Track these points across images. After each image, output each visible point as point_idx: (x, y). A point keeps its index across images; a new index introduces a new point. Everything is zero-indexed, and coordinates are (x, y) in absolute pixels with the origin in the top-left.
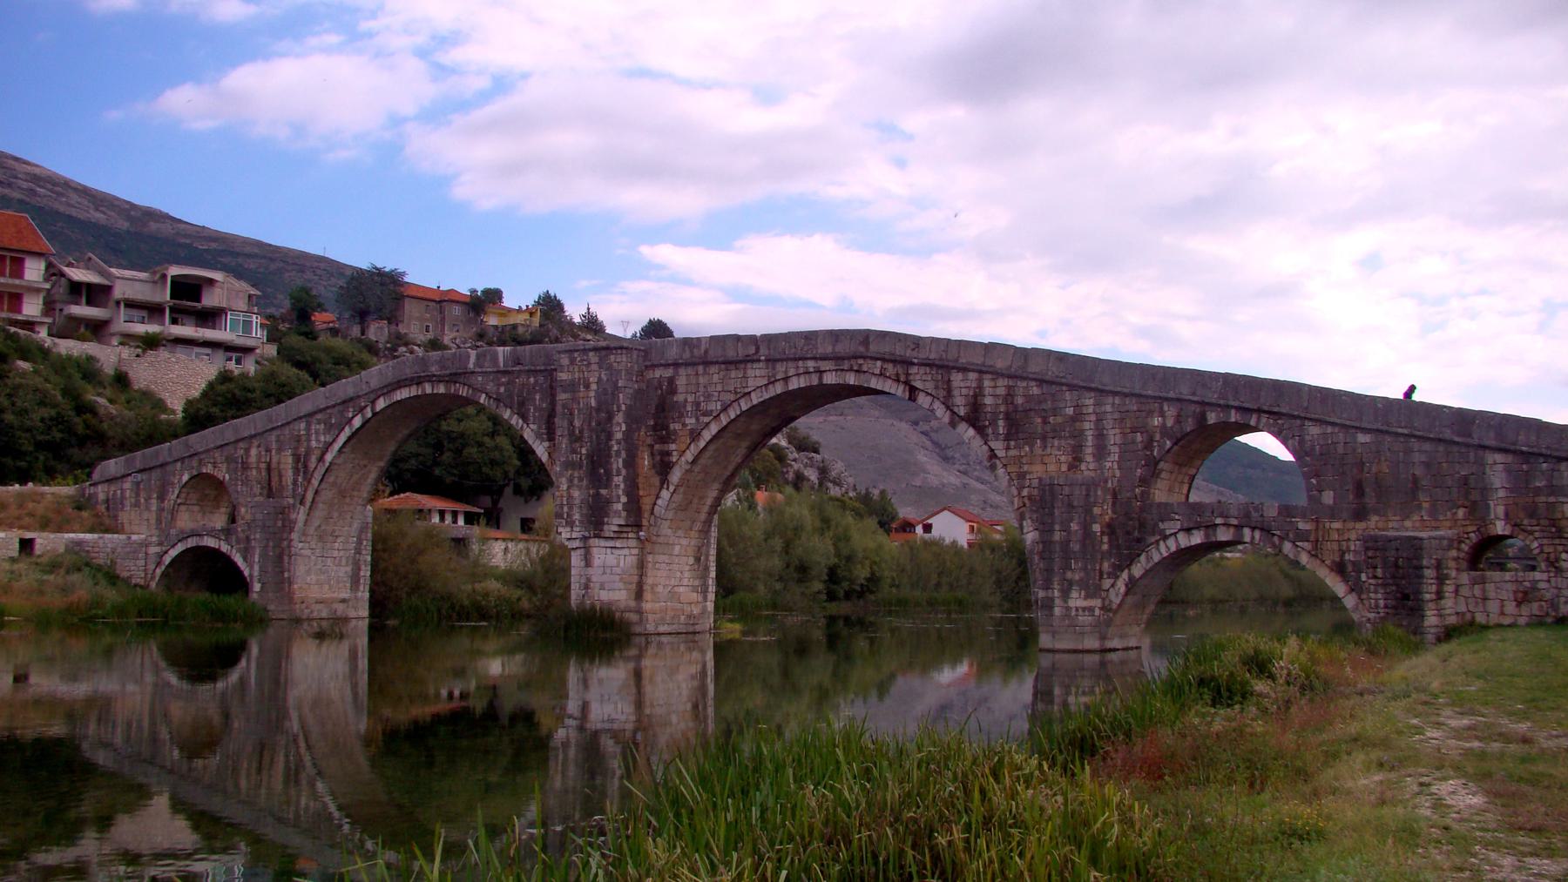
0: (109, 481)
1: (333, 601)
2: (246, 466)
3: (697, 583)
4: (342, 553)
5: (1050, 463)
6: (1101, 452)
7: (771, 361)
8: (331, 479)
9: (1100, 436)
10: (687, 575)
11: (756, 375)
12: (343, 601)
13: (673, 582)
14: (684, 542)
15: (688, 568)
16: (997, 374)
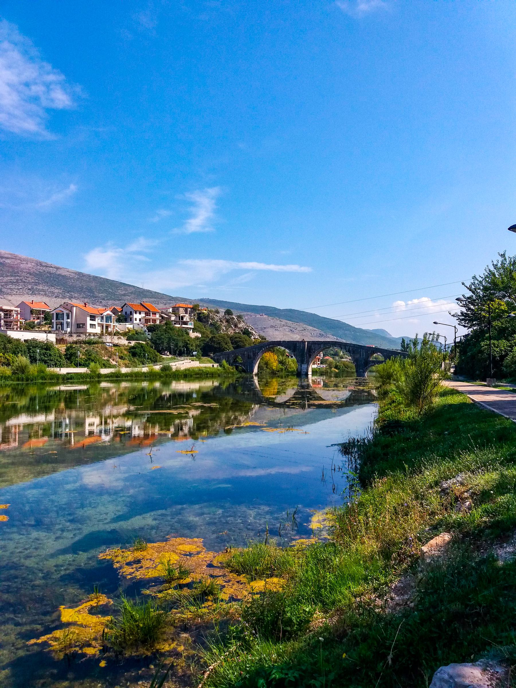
0: (218, 356)
2: (244, 354)
5: (357, 356)
6: (363, 355)
7: (324, 344)
9: (363, 354)
11: (322, 346)
16: (351, 347)
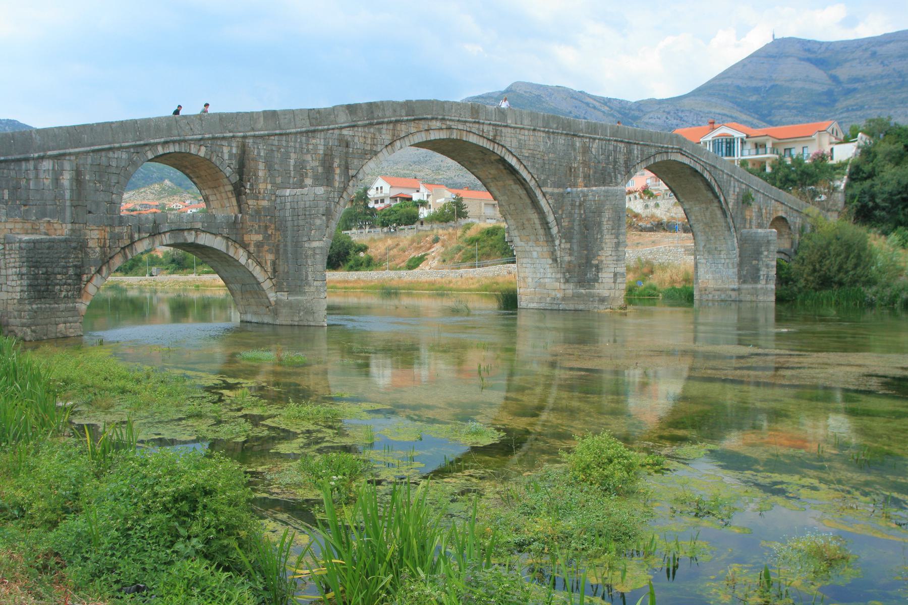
1: (726, 290)
3: (559, 276)
4: (727, 261)
8: (693, 218)
10: (549, 270)
12: (733, 290)
13: (538, 275)
14: (538, 249)
15: (548, 266)
